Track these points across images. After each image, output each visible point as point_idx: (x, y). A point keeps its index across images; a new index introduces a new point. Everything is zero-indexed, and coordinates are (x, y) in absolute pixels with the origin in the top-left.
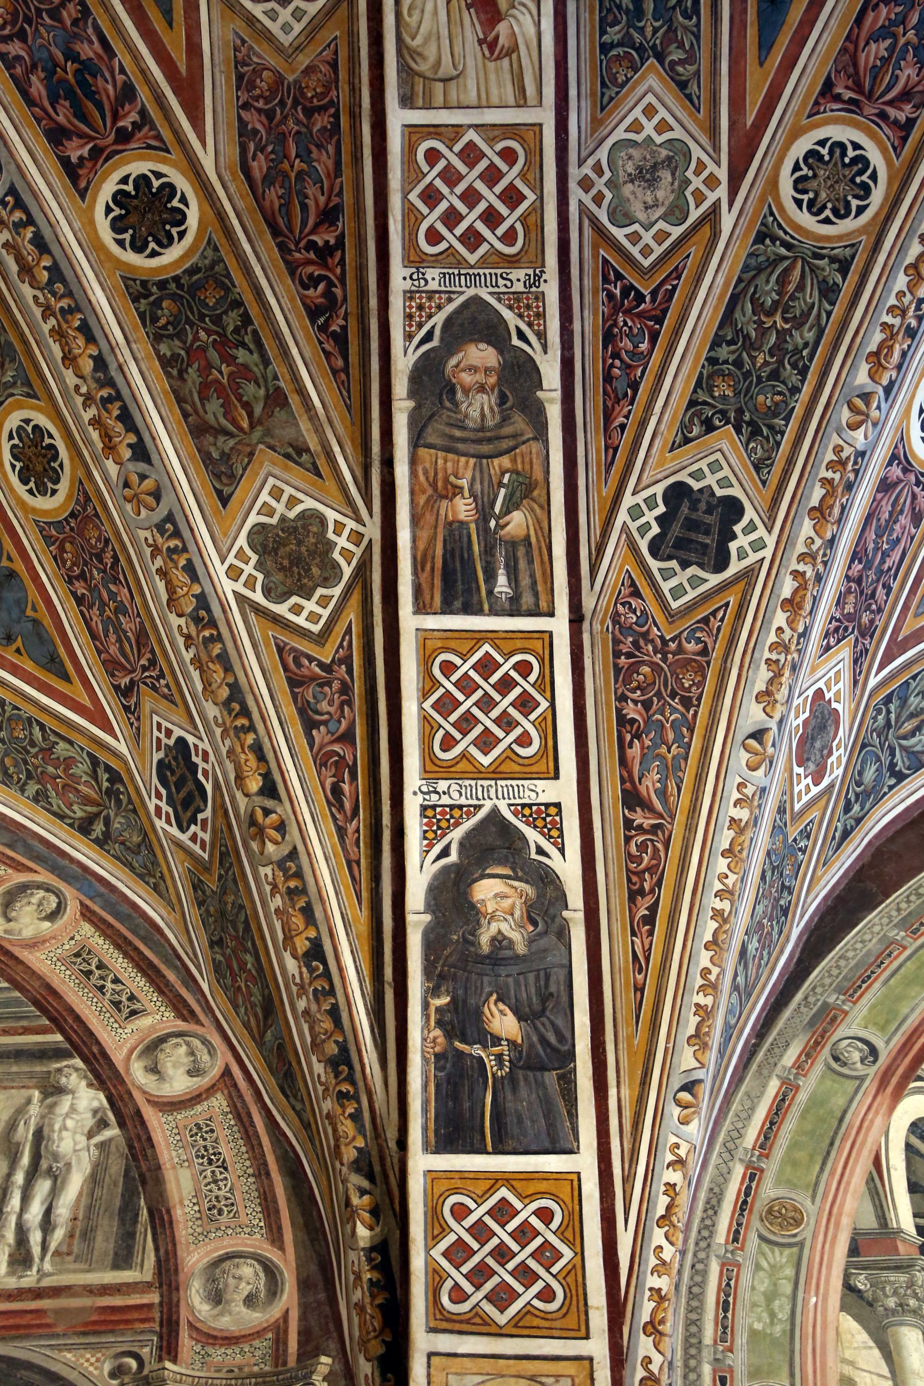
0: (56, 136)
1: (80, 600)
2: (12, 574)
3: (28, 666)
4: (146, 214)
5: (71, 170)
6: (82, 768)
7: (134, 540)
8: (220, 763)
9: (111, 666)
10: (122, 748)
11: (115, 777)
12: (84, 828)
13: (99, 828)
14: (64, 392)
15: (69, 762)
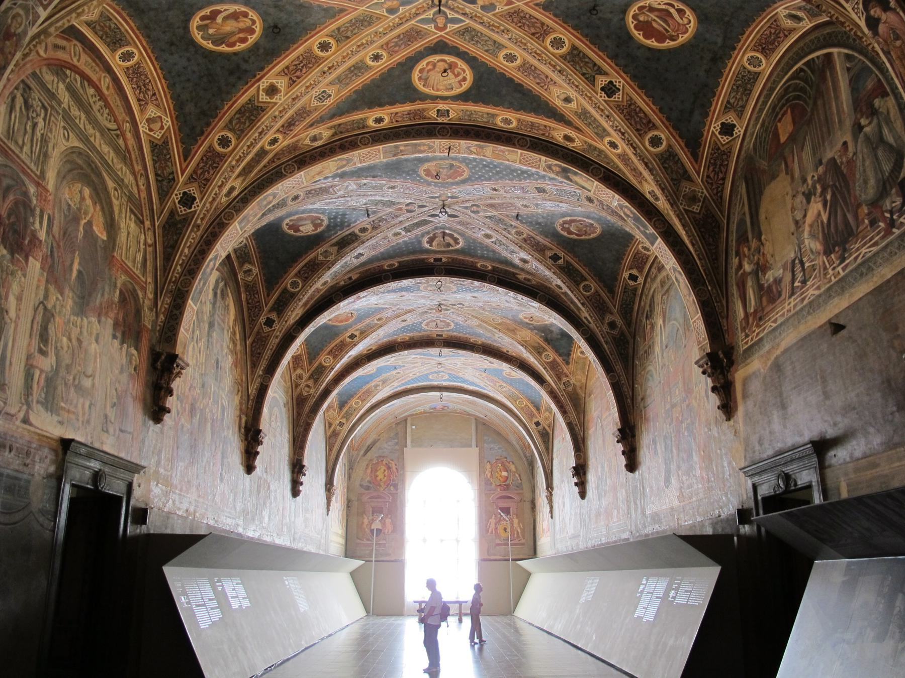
0: (283, 126)
1: (202, 159)
2: (197, 141)
3: (181, 150)
4: (274, 141)
5: (278, 130)
6: (169, 170)
7: (223, 173)
8: (201, 211)
9: (195, 172)
10: (181, 180)
11: (173, 179)
12: (157, 175)
13: (159, 178)
14: (242, 147)
15: (167, 166)
